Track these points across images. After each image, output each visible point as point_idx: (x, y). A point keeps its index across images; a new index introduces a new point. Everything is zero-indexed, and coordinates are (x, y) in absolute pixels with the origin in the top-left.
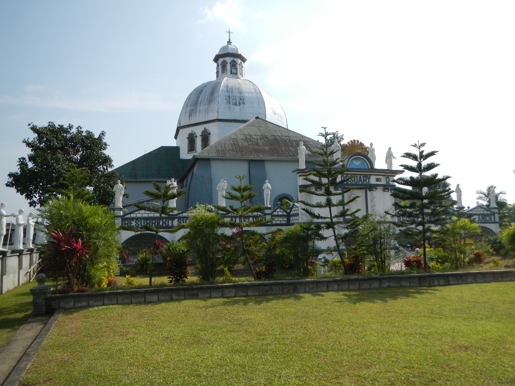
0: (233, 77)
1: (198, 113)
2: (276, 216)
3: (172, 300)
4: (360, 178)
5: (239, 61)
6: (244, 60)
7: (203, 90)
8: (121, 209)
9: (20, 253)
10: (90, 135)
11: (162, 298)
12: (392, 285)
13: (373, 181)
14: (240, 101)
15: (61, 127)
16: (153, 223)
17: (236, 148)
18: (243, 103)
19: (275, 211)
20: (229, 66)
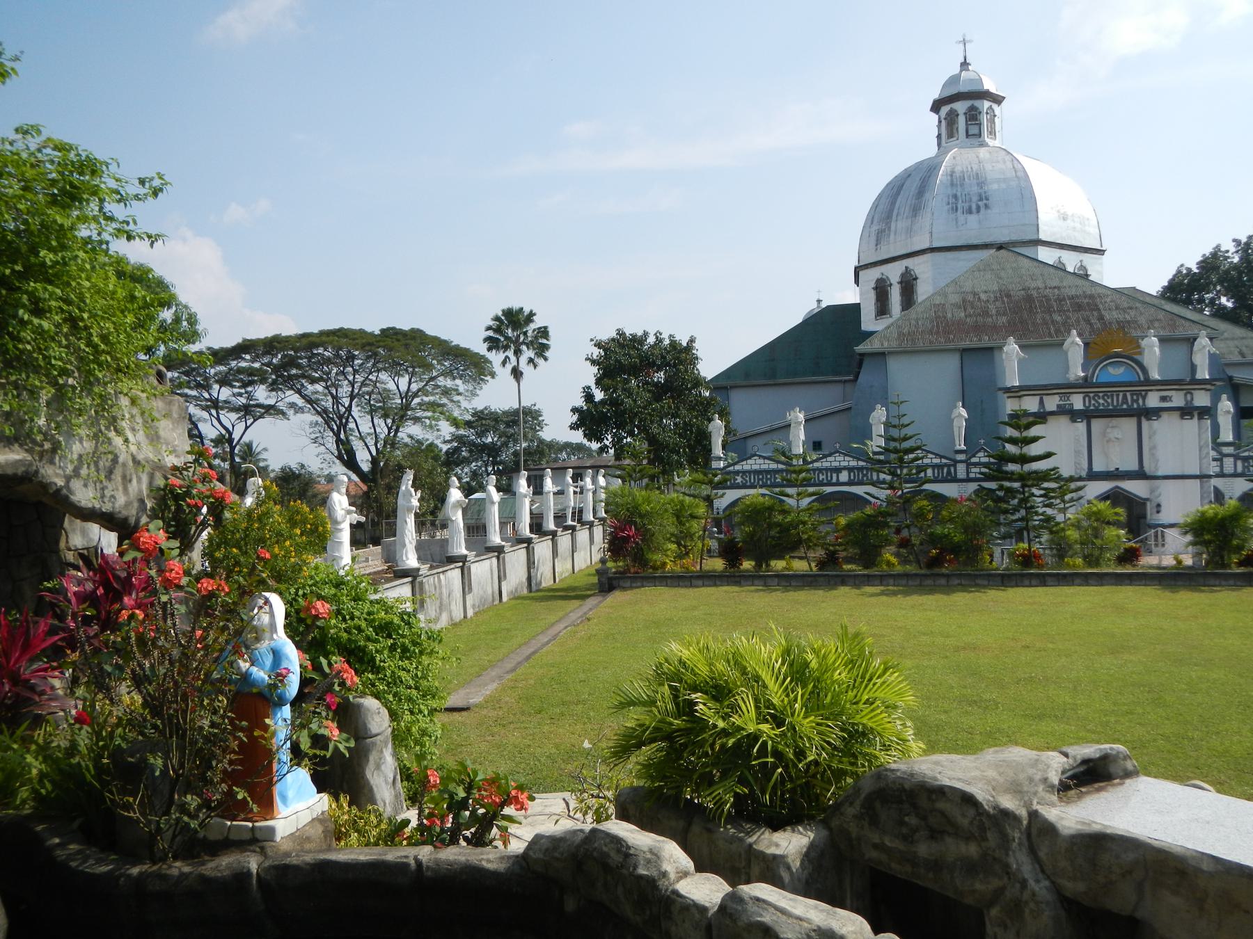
0: (972, 146)
1: (892, 236)
2: (975, 464)
3: (715, 585)
4: (1125, 397)
5: (987, 104)
6: (998, 100)
7: (903, 185)
8: (720, 459)
9: (591, 525)
10: (674, 344)
11: (706, 583)
12: (963, 582)
13: (1153, 401)
14: (980, 203)
15: (634, 336)
16: (767, 479)
17: (938, 326)
18: (986, 206)
19: (974, 456)
20: (961, 120)
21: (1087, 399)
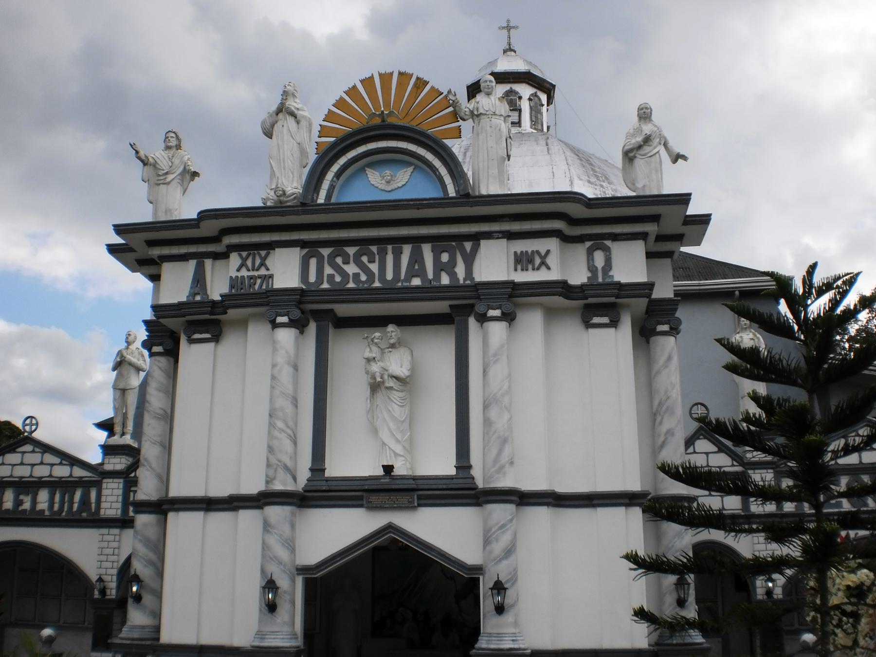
4: (417, 258)
21: (313, 262)
